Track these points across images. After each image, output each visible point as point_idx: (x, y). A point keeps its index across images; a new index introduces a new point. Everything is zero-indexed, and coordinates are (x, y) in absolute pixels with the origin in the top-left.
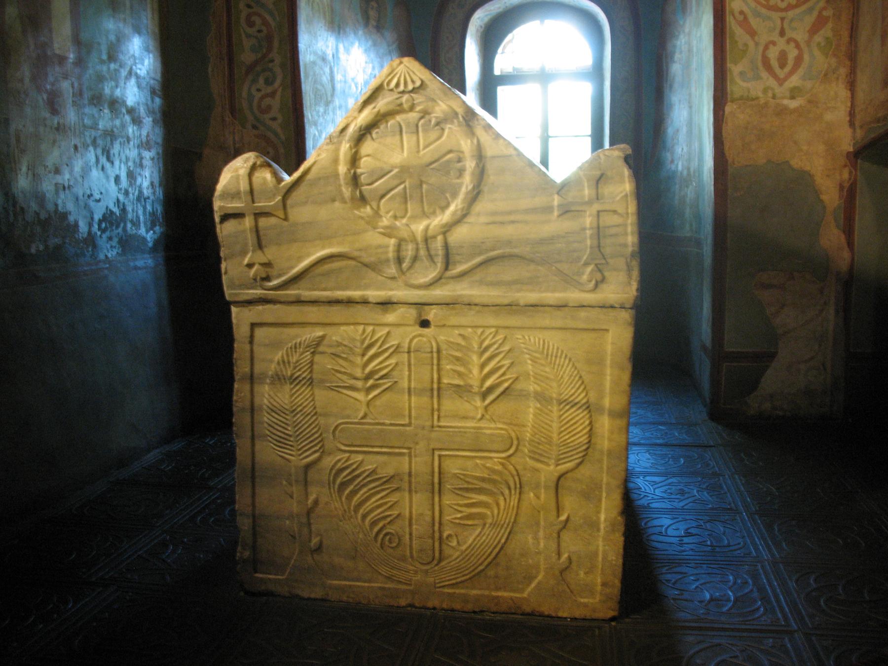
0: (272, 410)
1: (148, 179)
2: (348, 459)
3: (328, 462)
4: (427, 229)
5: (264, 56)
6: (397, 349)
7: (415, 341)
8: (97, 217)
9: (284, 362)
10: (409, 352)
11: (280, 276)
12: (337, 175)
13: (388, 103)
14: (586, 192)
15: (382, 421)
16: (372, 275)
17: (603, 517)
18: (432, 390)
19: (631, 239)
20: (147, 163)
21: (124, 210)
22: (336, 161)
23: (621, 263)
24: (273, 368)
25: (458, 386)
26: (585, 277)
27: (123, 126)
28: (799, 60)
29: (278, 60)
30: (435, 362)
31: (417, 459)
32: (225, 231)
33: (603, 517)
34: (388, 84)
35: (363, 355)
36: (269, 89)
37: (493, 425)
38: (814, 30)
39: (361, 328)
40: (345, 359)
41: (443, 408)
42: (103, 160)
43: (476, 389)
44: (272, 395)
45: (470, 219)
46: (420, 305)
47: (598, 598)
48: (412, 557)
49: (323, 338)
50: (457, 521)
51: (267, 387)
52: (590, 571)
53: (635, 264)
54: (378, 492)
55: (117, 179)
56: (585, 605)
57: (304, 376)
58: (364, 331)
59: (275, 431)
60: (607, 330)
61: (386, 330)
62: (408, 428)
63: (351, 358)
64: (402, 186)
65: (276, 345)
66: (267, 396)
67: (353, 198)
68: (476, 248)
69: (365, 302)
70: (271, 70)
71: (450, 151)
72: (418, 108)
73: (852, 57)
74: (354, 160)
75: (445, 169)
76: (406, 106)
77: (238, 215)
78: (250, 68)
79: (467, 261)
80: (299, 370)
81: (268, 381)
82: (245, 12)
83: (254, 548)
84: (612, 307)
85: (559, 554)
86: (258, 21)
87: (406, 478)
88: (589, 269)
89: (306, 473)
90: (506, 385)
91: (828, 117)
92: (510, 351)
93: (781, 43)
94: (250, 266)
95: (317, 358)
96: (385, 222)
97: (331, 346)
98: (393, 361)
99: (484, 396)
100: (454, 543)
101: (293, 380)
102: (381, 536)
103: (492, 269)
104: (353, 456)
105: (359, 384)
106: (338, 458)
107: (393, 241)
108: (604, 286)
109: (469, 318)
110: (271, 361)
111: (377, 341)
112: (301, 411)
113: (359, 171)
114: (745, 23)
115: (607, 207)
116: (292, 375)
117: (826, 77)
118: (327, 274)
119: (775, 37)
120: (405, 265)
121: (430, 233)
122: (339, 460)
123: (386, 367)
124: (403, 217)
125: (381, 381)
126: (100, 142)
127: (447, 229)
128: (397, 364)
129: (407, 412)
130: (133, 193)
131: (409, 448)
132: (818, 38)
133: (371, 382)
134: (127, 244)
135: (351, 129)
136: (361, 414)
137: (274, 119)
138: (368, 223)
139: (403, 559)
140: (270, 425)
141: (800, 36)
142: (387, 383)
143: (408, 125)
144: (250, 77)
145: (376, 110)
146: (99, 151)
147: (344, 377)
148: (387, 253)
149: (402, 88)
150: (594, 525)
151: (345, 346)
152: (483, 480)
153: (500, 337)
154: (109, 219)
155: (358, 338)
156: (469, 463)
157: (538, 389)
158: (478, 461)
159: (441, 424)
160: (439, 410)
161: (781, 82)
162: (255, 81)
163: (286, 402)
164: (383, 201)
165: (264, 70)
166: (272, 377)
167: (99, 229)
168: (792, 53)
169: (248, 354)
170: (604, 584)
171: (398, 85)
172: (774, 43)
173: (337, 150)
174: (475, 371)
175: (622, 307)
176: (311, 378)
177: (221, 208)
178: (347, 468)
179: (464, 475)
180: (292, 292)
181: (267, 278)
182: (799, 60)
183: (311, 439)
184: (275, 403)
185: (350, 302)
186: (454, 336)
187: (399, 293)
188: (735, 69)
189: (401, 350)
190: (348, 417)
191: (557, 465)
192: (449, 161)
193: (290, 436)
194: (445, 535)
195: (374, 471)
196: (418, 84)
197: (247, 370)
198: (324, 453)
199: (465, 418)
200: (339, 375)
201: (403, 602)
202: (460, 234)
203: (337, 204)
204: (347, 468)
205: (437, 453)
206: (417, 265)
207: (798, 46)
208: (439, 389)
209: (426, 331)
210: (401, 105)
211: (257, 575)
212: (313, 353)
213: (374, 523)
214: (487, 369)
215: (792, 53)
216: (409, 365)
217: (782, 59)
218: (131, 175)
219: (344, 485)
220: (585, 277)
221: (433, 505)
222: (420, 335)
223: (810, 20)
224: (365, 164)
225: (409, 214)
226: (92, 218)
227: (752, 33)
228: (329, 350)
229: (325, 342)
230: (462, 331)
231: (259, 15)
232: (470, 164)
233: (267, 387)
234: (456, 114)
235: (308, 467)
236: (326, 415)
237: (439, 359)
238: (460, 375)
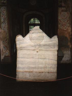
5: (4, 21)
23: (57, 46)
28: (66, 25)
29: (6, 22)
38: (67, 21)
70: (5, 23)
82: (2, 15)
86: (4, 16)
91: (69, 31)
117: (69, 27)
132: (68, 22)
141: (66, 22)
144: (2, 24)
162: (3, 24)
165: (4, 23)
182: (66, 25)
217: (64, 24)
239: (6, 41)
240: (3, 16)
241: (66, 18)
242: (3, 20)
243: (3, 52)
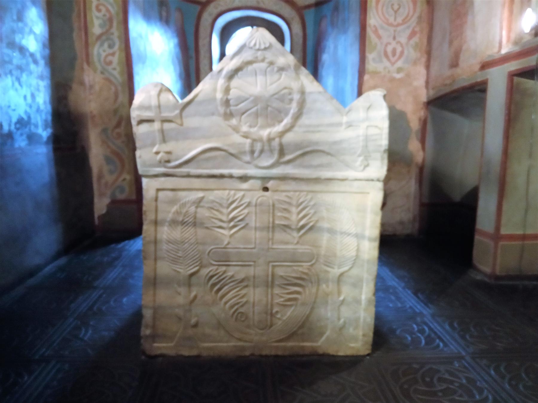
0: (169, 242)
1: (43, 98)
2: (217, 269)
3: (205, 272)
4: (270, 134)
6: (249, 205)
7: (260, 199)
8: (14, 120)
9: (178, 213)
10: (256, 205)
11: (176, 160)
15: (238, 246)
16: (234, 160)
17: (363, 297)
19: (384, 142)
20: (42, 89)
21: (29, 118)
22: (215, 90)
23: (378, 155)
24: (170, 216)
25: (285, 226)
26: (358, 163)
27: (28, 64)
28: (402, 53)
30: (271, 211)
32: (139, 131)
35: (228, 207)
36: (111, 51)
38: (410, 37)
39: (227, 192)
40: (217, 210)
42: (17, 84)
45: (296, 129)
46: (265, 179)
49: (203, 198)
50: (281, 303)
51: (166, 228)
52: (356, 328)
53: (386, 156)
54: (235, 288)
55: (25, 97)
56: (353, 348)
57: (190, 220)
58: (229, 194)
59: (171, 255)
60: (368, 193)
62: (254, 250)
65: (172, 202)
68: (298, 146)
69: (231, 177)
71: (285, 88)
72: (267, 61)
73: (429, 53)
74: (227, 90)
75: (282, 99)
77: (149, 121)
78: (99, 37)
79: (292, 153)
80: (188, 217)
81: (167, 224)
83: (154, 327)
84: (372, 180)
85: (339, 319)
86: (103, 10)
87: (252, 279)
88: (361, 158)
90: (311, 224)
92: (314, 205)
93: (394, 44)
94: (157, 153)
95: (199, 210)
98: (246, 211)
100: (279, 316)
101: (183, 223)
102: (236, 314)
103: (307, 158)
104: (220, 267)
107: (248, 141)
108: (368, 169)
109: (293, 186)
110: (169, 212)
111: (236, 200)
112: (188, 242)
113: (229, 97)
114: (376, 31)
116: (183, 220)
117: (415, 63)
118: (208, 159)
119: (391, 40)
120: (256, 154)
121: (272, 136)
122: (210, 271)
123: (241, 215)
124: (255, 126)
126: (14, 72)
127: (282, 134)
128: (248, 213)
130: (34, 109)
131: (254, 262)
132: (412, 42)
134: (32, 138)
135: (224, 72)
137: (114, 69)
139: (248, 327)
141: (403, 39)
142: (242, 224)
146: (14, 78)
150: (358, 301)
154: (22, 123)
156: (289, 269)
161: (393, 64)
162: (102, 45)
164: (243, 117)
165: (108, 39)
167: (16, 128)
168: (399, 49)
170: (364, 335)
171: (255, 45)
173: (216, 84)
175: (378, 180)
177: (138, 116)
178: (215, 275)
179: (287, 276)
180: (184, 170)
181: (168, 161)
182: (402, 53)
183: (194, 258)
185: (222, 176)
186: (282, 197)
187: (251, 171)
188: (370, 56)
190: (218, 244)
192: (284, 95)
193: (180, 257)
194: (274, 311)
195: (232, 277)
196: (267, 45)
198: (202, 266)
199: (287, 243)
201: (247, 353)
202: (289, 137)
204: (215, 275)
206: (263, 155)
207: (402, 45)
209: (266, 194)
210: (257, 57)
212: (197, 207)
213: (232, 307)
214: (301, 215)
215: (399, 49)
216: (256, 213)
218: (33, 96)
219: (214, 285)
220: (358, 163)
221: (267, 294)
222: (263, 196)
223: (408, 32)
224: (233, 93)
225: (259, 125)
226: (11, 121)
227: (379, 37)
228: (207, 205)
229: (205, 200)
231: (104, 5)
232: (296, 97)
233: (166, 228)
236: (204, 244)
237: (273, 210)
238: (286, 218)
239: (118, 130)
240: (101, 7)
241: (403, 20)
242: (101, 26)
243: (103, 181)
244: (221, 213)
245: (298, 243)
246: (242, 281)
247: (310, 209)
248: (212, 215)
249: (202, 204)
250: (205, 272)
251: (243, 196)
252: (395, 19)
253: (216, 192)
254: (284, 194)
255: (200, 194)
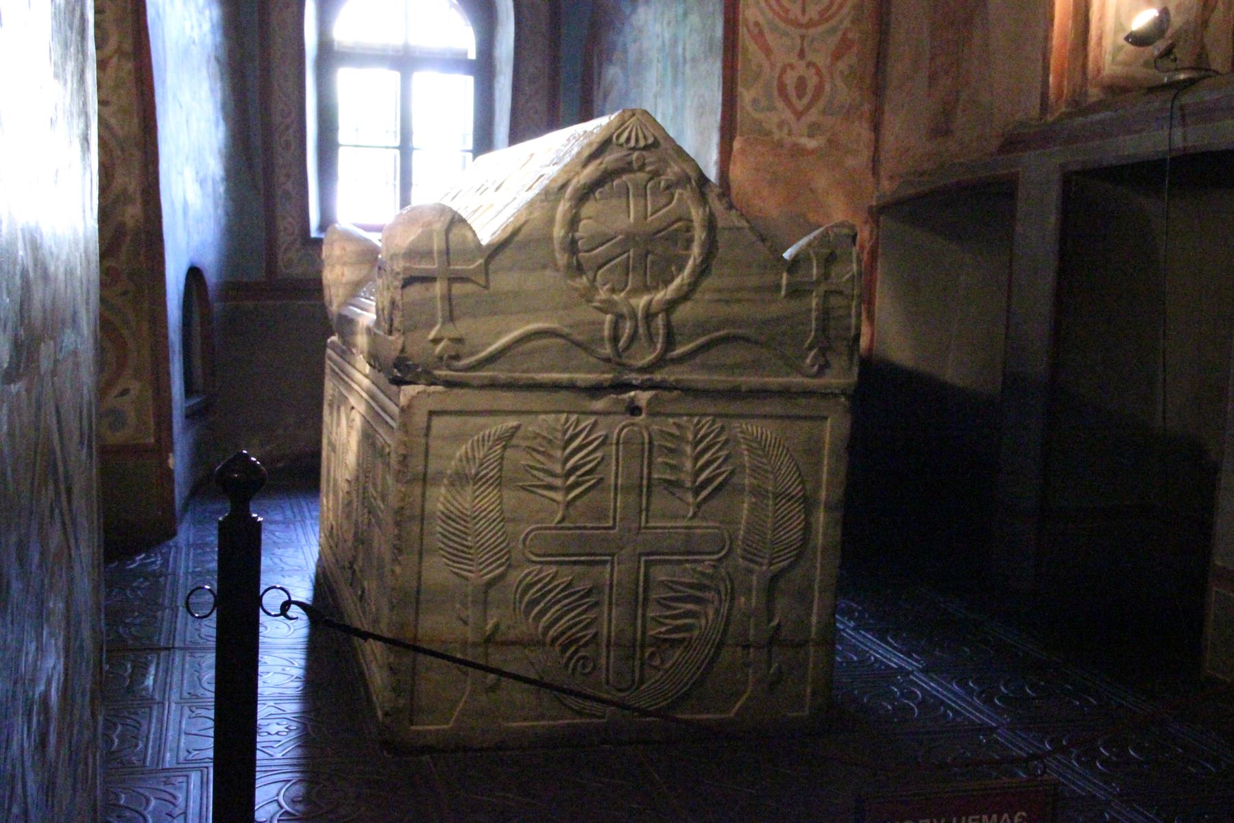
2: (540, 571)
3: (515, 576)
4: (650, 303)
7: (625, 431)
11: (472, 354)
12: (550, 239)
13: (617, 160)
14: (815, 271)
17: (814, 619)
18: (641, 486)
22: (551, 221)
25: (669, 482)
28: (819, 89)
31: (623, 567)
33: (814, 619)
34: (618, 137)
35: (564, 448)
37: (704, 524)
38: (837, 56)
39: (564, 416)
40: (543, 453)
41: (652, 507)
43: (688, 485)
44: (450, 497)
45: (697, 296)
47: (807, 712)
48: (608, 683)
49: (518, 428)
58: (567, 420)
59: (451, 544)
61: (592, 419)
62: (612, 532)
63: (552, 452)
64: (625, 255)
65: (458, 438)
66: (442, 499)
67: (569, 266)
68: (701, 327)
72: (648, 168)
73: (878, 90)
74: (573, 222)
75: (672, 239)
76: (635, 166)
81: (445, 481)
89: (486, 592)
90: (721, 479)
92: (727, 442)
93: (801, 69)
94: (436, 341)
95: (509, 453)
96: (603, 294)
97: (526, 438)
98: (599, 454)
99: (697, 491)
101: (476, 479)
105: (558, 482)
106: (526, 571)
107: (609, 317)
114: (759, 37)
115: (833, 288)
116: (477, 474)
119: (793, 59)
120: (622, 344)
121: (653, 309)
122: (527, 575)
124: (623, 290)
125: (587, 478)
127: (671, 306)
128: (603, 458)
129: (611, 513)
132: (841, 65)
133: (572, 479)
136: (559, 517)
138: (582, 296)
140: (445, 536)
141: (822, 60)
143: (636, 186)
145: (603, 166)
147: (541, 475)
148: (602, 330)
149: (632, 143)
151: (544, 438)
152: (691, 586)
153: (718, 425)
155: (559, 427)
156: (677, 569)
157: (755, 482)
158: (688, 565)
159: (651, 524)
160: (647, 510)
161: (799, 115)
163: (467, 506)
164: (600, 272)
166: (451, 476)
168: (813, 81)
169: (423, 448)
171: (628, 139)
172: (792, 67)
173: (554, 209)
174: (688, 465)
176: (500, 477)
178: (536, 583)
179: (672, 582)
180: (486, 374)
181: (457, 357)
182: (819, 89)
184: (452, 509)
188: (746, 96)
189: (608, 441)
191: (771, 564)
196: (650, 141)
197: (420, 468)
199: (675, 517)
200: (535, 472)
203: (548, 272)
205: (643, 559)
206: (635, 346)
207: (818, 72)
208: (649, 487)
210: (630, 163)
211: (413, 728)
214: (700, 463)
215: (813, 81)
217: (801, 84)
219: (534, 602)
220: (808, 361)
223: (833, 41)
225: (628, 288)
227: (767, 51)
229: (520, 433)
230: (677, 420)
232: (699, 235)
233: (443, 490)
234: (689, 179)
235: (490, 584)
241: (821, 14)
244: (550, 456)
245: (695, 515)
246: (589, 593)
247: (720, 449)
248: (531, 463)
249: (514, 442)
250: (515, 576)
251: (595, 424)
252: (804, 11)
253: (542, 417)
254: (671, 420)
255: (512, 422)
